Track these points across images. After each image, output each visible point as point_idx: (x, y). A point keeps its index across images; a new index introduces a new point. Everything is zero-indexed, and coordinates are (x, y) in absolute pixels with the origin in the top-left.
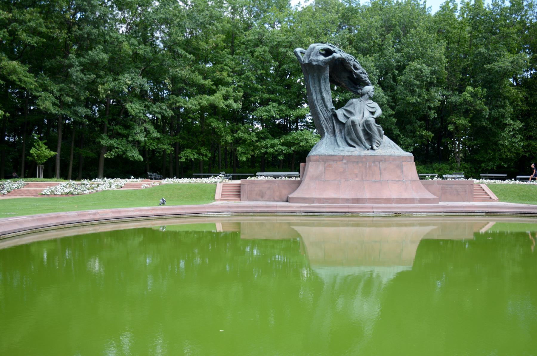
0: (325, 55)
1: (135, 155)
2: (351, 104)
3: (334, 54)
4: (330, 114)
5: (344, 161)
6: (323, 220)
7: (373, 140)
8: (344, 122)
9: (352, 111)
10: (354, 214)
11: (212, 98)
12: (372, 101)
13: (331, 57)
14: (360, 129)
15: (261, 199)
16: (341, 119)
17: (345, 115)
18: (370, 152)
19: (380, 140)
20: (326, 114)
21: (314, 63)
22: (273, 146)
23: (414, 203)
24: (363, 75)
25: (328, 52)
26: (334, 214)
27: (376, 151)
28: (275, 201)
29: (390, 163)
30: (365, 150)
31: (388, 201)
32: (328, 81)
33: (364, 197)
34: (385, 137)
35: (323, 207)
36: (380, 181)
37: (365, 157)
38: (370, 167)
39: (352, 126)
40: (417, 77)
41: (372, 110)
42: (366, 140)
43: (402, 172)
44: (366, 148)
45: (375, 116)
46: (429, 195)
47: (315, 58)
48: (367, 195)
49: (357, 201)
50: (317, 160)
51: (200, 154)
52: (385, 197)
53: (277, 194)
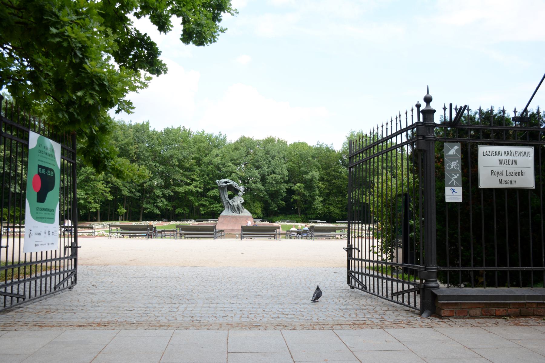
1: (157, 211)
10: (230, 234)
11: (189, 187)
14: (236, 207)
16: (231, 203)
18: (239, 215)
22: (216, 208)
25: (226, 182)
40: (274, 180)
48: (236, 228)
49: (233, 230)
51: (184, 210)
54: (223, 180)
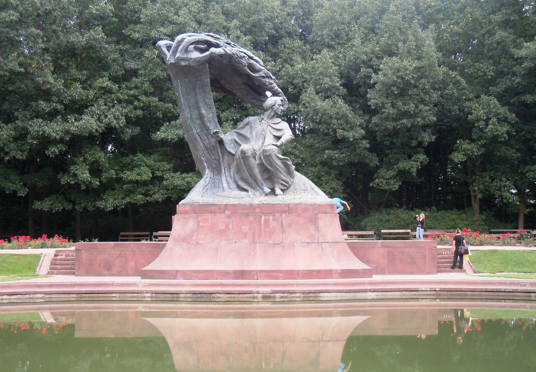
0: (202, 51)
2: (248, 124)
3: (213, 50)
4: (213, 141)
5: (228, 212)
6: (183, 308)
7: (276, 180)
8: (234, 153)
9: (248, 135)
12: (280, 120)
13: (207, 53)
14: (255, 163)
15: (106, 272)
17: (236, 142)
19: (288, 180)
20: (207, 141)
21: (183, 63)
23: (332, 278)
24: (268, 80)
26: (199, 297)
27: (279, 196)
28: (128, 275)
29: (299, 215)
30: (261, 195)
31: (291, 274)
32: (208, 88)
33: (251, 269)
34: (297, 175)
35: (183, 285)
36: (281, 244)
37: (260, 206)
38: (267, 222)
39: (243, 158)
41: (278, 134)
42: (265, 180)
43: (317, 229)
44: (264, 192)
45: (279, 143)
46: (357, 265)
47: (184, 56)
48: (258, 265)
49: (242, 274)
50: (186, 212)
52: (285, 268)
53: (132, 264)
54: (188, 37)
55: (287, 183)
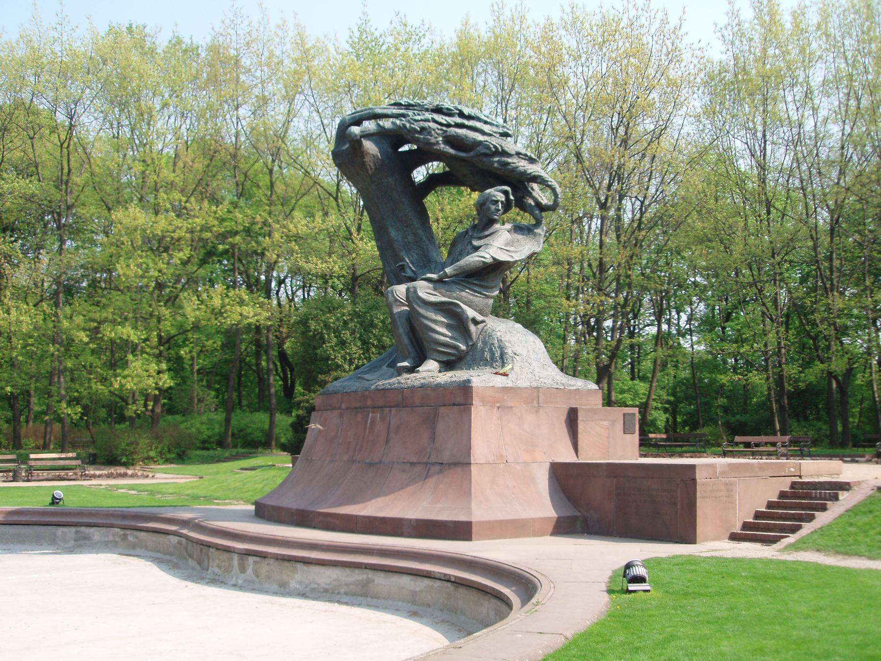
24: (496, 159)
43: (433, 437)
55: (456, 348)
